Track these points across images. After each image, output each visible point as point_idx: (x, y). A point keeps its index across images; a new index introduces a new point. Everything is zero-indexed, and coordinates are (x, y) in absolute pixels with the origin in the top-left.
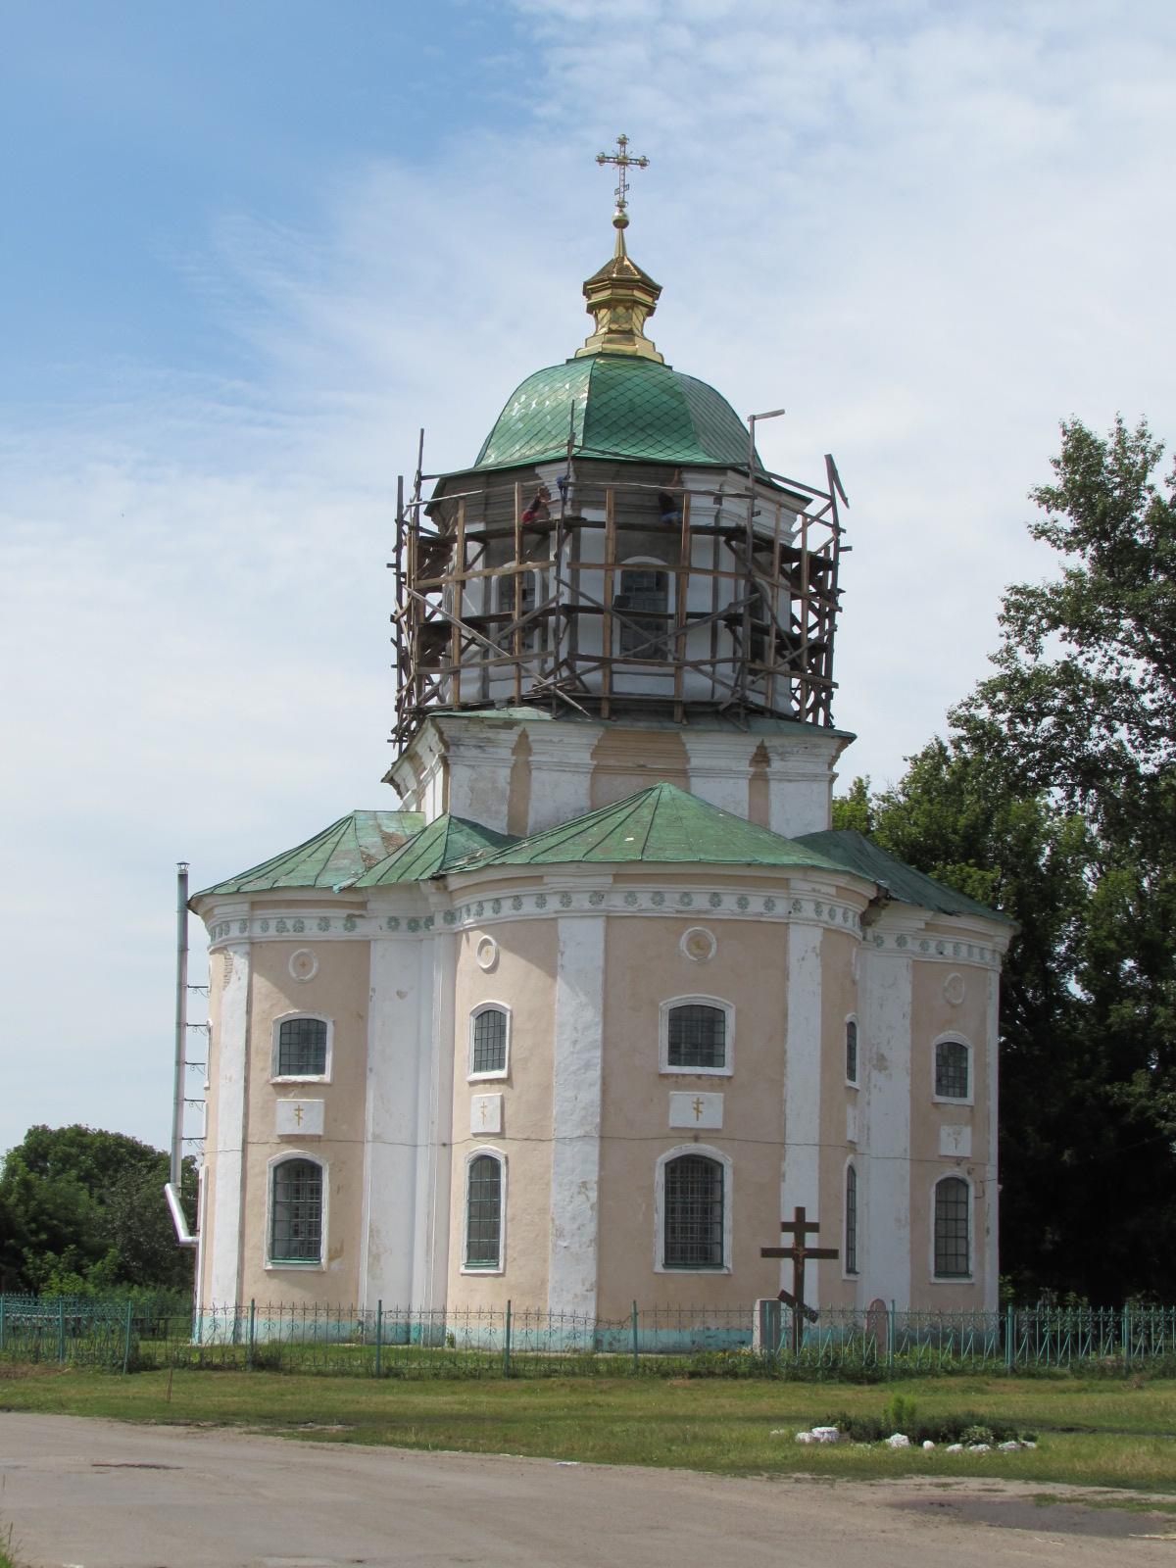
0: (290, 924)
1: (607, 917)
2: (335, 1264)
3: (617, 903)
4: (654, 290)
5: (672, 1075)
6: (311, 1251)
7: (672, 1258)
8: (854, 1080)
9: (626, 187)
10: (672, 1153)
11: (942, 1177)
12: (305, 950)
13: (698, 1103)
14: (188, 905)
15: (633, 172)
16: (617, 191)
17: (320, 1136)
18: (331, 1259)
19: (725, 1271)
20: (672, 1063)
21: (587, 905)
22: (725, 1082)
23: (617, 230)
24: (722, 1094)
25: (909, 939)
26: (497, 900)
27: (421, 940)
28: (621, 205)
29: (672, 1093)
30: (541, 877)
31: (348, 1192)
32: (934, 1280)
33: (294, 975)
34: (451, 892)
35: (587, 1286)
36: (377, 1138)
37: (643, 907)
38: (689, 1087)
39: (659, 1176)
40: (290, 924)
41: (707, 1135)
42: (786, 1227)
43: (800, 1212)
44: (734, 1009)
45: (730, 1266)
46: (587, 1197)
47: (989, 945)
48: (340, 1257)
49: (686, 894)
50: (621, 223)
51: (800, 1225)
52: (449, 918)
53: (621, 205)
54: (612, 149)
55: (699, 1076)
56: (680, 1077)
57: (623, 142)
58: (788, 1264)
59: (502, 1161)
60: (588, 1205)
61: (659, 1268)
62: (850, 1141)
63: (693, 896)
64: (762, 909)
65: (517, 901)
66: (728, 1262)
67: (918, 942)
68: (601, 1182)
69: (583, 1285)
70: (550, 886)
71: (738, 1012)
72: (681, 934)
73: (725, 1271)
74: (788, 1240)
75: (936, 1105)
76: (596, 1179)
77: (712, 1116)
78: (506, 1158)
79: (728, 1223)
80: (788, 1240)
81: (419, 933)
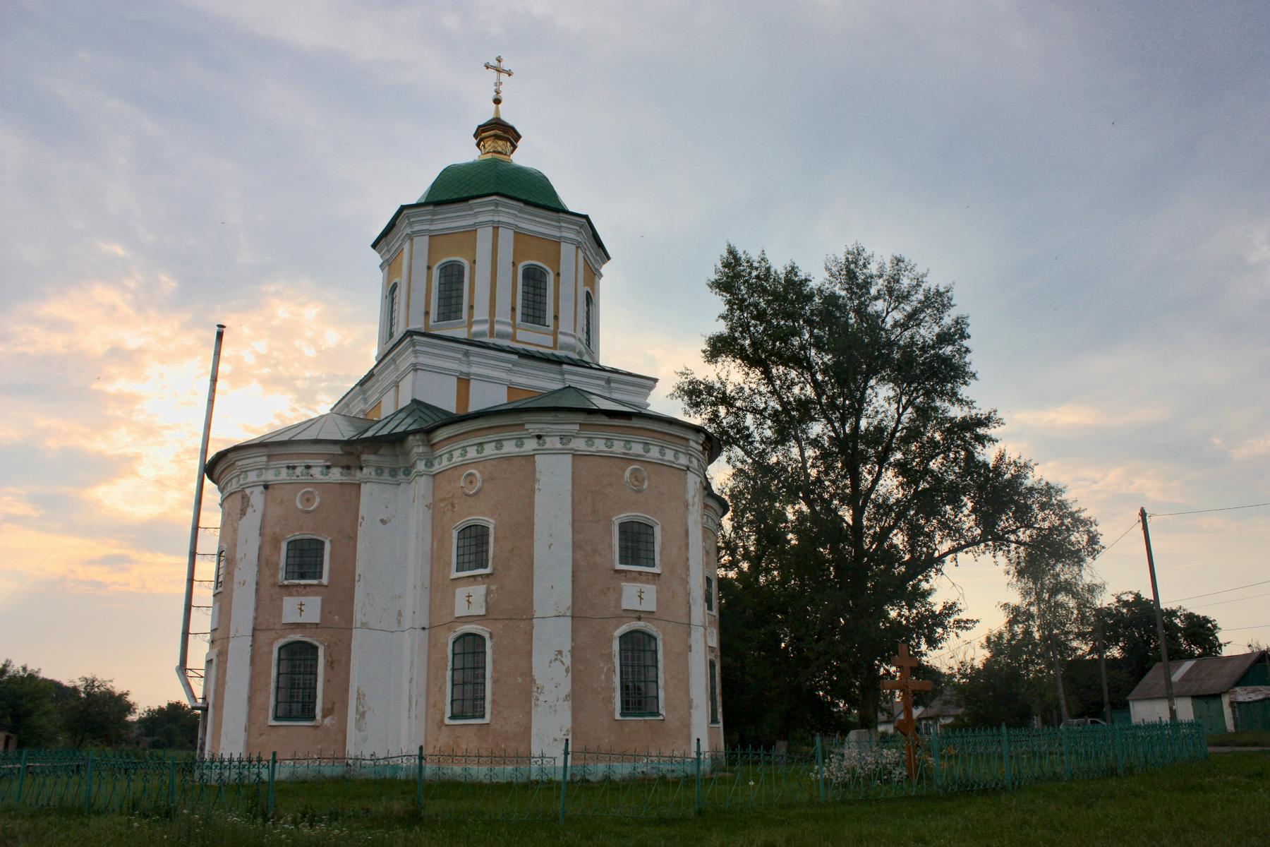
2: (327, 721)
3: (579, 444)
4: (518, 137)
6: (307, 712)
7: (628, 709)
9: (501, 83)
10: (624, 629)
12: (310, 489)
14: (213, 468)
15: (504, 77)
16: (496, 84)
17: (317, 624)
18: (324, 716)
19: (661, 718)
20: (621, 563)
21: (559, 446)
23: (495, 105)
24: (654, 587)
26: (481, 444)
27: (399, 485)
29: (623, 584)
30: (523, 425)
31: (340, 664)
33: (300, 506)
34: (433, 445)
36: (364, 625)
37: (600, 449)
38: (634, 580)
39: (616, 646)
44: (660, 526)
45: (664, 714)
46: (562, 661)
48: (331, 714)
50: (497, 101)
52: (429, 464)
53: (498, 93)
54: (494, 63)
55: (640, 573)
59: (487, 636)
60: (564, 668)
61: (618, 717)
65: (499, 443)
66: (662, 711)
68: (573, 651)
69: (561, 731)
70: (530, 431)
71: (663, 529)
72: (625, 470)
73: (661, 718)
76: (570, 648)
77: (650, 604)
81: (399, 478)
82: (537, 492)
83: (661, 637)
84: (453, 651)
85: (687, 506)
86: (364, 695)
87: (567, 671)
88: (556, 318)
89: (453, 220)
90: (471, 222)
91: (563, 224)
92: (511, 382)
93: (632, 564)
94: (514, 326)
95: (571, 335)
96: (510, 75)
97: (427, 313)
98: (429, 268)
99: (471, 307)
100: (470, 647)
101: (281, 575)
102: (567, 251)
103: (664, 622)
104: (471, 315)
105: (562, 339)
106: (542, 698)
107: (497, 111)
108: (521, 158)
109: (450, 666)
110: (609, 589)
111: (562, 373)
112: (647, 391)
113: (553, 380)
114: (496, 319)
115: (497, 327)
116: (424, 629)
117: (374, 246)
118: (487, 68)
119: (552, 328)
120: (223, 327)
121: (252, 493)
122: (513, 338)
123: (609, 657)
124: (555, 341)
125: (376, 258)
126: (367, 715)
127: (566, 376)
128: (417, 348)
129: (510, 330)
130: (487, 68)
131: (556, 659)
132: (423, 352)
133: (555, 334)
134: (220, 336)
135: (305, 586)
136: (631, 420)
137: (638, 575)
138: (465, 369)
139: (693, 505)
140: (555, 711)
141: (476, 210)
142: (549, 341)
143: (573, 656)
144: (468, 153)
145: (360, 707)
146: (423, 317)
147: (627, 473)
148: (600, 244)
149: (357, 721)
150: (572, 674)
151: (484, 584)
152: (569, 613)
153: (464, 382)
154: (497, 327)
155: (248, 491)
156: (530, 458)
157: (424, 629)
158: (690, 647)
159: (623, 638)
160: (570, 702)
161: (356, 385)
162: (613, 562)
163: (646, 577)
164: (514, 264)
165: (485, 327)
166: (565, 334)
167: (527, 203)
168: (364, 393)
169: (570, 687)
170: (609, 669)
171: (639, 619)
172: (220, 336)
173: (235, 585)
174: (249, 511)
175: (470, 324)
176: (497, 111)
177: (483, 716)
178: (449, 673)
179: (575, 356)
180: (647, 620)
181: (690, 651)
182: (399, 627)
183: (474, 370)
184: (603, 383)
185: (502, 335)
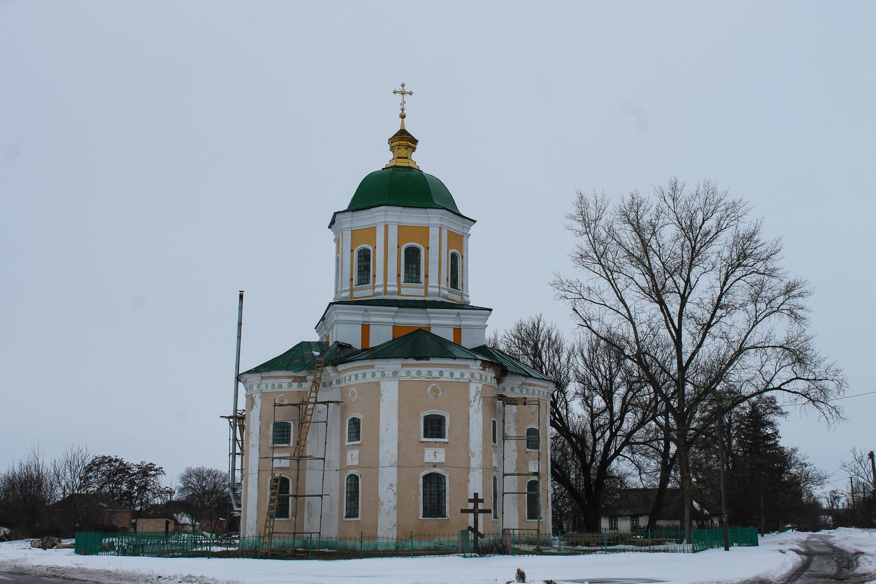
0: (276, 385)
1: (399, 381)
4: (415, 141)
5: (425, 442)
8: (495, 443)
10: (426, 472)
11: (528, 481)
12: (282, 395)
13: (435, 452)
14: (238, 378)
15: (407, 97)
18: (293, 516)
19: (447, 518)
20: (425, 436)
22: (446, 444)
25: (516, 389)
28: (403, 110)
32: (527, 520)
35: (393, 525)
38: (432, 446)
39: (421, 482)
40: (276, 385)
41: (440, 465)
42: (470, 501)
43: (476, 495)
45: (448, 516)
46: (392, 490)
47: (546, 391)
49: (430, 372)
51: (476, 500)
53: (403, 110)
54: (399, 88)
55: (435, 442)
56: (428, 443)
57: (403, 86)
58: (471, 516)
59: (359, 476)
61: (421, 517)
62: (494, 467)
63: (432, 372)
64: (459, 377)
66: (448, 515)
67: (519, 390)
68: (398, 485)
72: (428, 387)
73: (447, 518)
74: (471, 506)
75: (527, 452)
76: (396, 482)
77: (441, 457)
78: (361, 475)
79: (447, 499)
80: (471, 506)
82: (381, 401)
83: (448, 476)
84: (347, 483)
85: (469, 402)
86: (312, 505)
87: (395, 494)
88: (427, 276)
91: (430, 215)
92: (395, 323)
93: (430, 438)
94: (399, 286)
96: (411, 94)
97: (352, 280)
98: (352, 251)
99: (375, 276)
100: (354, 481)
101: (271, 441)
102: (434, 233)
103: (450, 468)
105: (430, 290)
106: (382, 508)
107: (403, 124)
109: (345, 491)
110: (417, 451)
111: (428, 313)
112: (485, 317)
113: (423, 318)
115: (389, 289)
116: (337, 470)
117: (330, 227)
118: (395, 93)
119: (423, 284)
120: (243, 292)
121: (255, 397)
122: (399, 293)
123: (418, 486)
124: (426, 291)
125: (331, 235)
126: (313, 515)
127: (430, 315)
128: (337, 311)
129: (396, 289)
130: (395, 93)
131: (389, 489)
132: (340, 313)
134: (241, 297)
135: (282, 447)
136: (429, 360)
137: (434, 443)
138: (366, 319)
139: (474, 401)
140: (389, 514)
141: (375, 215)
142: (422, 292)
143: (398, 487)
145: (309, 511)
146: (349, 282)
147: (429, 389)
149: (308, 518)
150: (397, 496)
151: (358, 449)
152: (396, 465)
153: (366, 328)
154: (389, 289)
155: (254, 396)
156: (378, 384)
157: (337, 470)
158: (469, 480)
159: (425, 477)
160: (396, 510)
161: (320, 321)
162: (420, 437)
163: (439, 444)
164: (398, 246)
165: (381, 289)
166: (432, 287)
167: (403, 207)
168: (325, 325)
169: (396, 502)
170: (416, 493)
171: (435, 466)
172: (241, 297)
173: (250, 447)
174: (255, 406)
175: (374, 288)
176: (403, 124)
177: (357, 517)
178: (345, 494)
179: (439, 299)
180: (439, 467)
181: (469, 482)
182: (328, 469)
183: (372, 319)
184: (455, 316)
185: (392, 293)
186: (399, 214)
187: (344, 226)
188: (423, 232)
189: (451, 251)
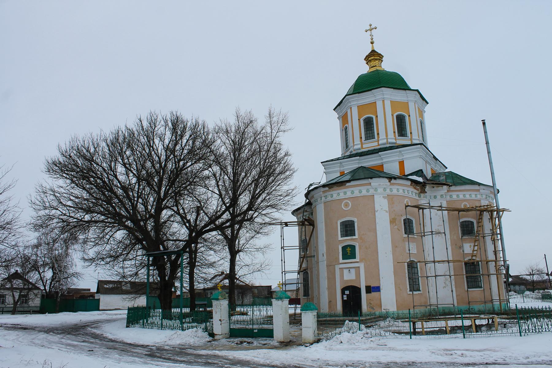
28: (372, 39)
50: (372, 43)
54: (368, 28)
89: (366, 98)
90: (374, 99)
94: (396, 139)
95: (417, 139)
97: (361, 138)
99: (378, 134)
102: (411, 106)
104: (378, 137)
107: (373, 47)
108: (387, 66)
114: (388, 137)
117: (334, 110)
119: (410, 137)
125: (335, 115)
133: (411, 139)
144: (365, 69)
148: (423, 99)
167: (394, 88)
175: (378, 141)
176: (373, 47)
186: (391, 93)
187: (352, 104)
188: (406, 105)
189: (420, 118)
